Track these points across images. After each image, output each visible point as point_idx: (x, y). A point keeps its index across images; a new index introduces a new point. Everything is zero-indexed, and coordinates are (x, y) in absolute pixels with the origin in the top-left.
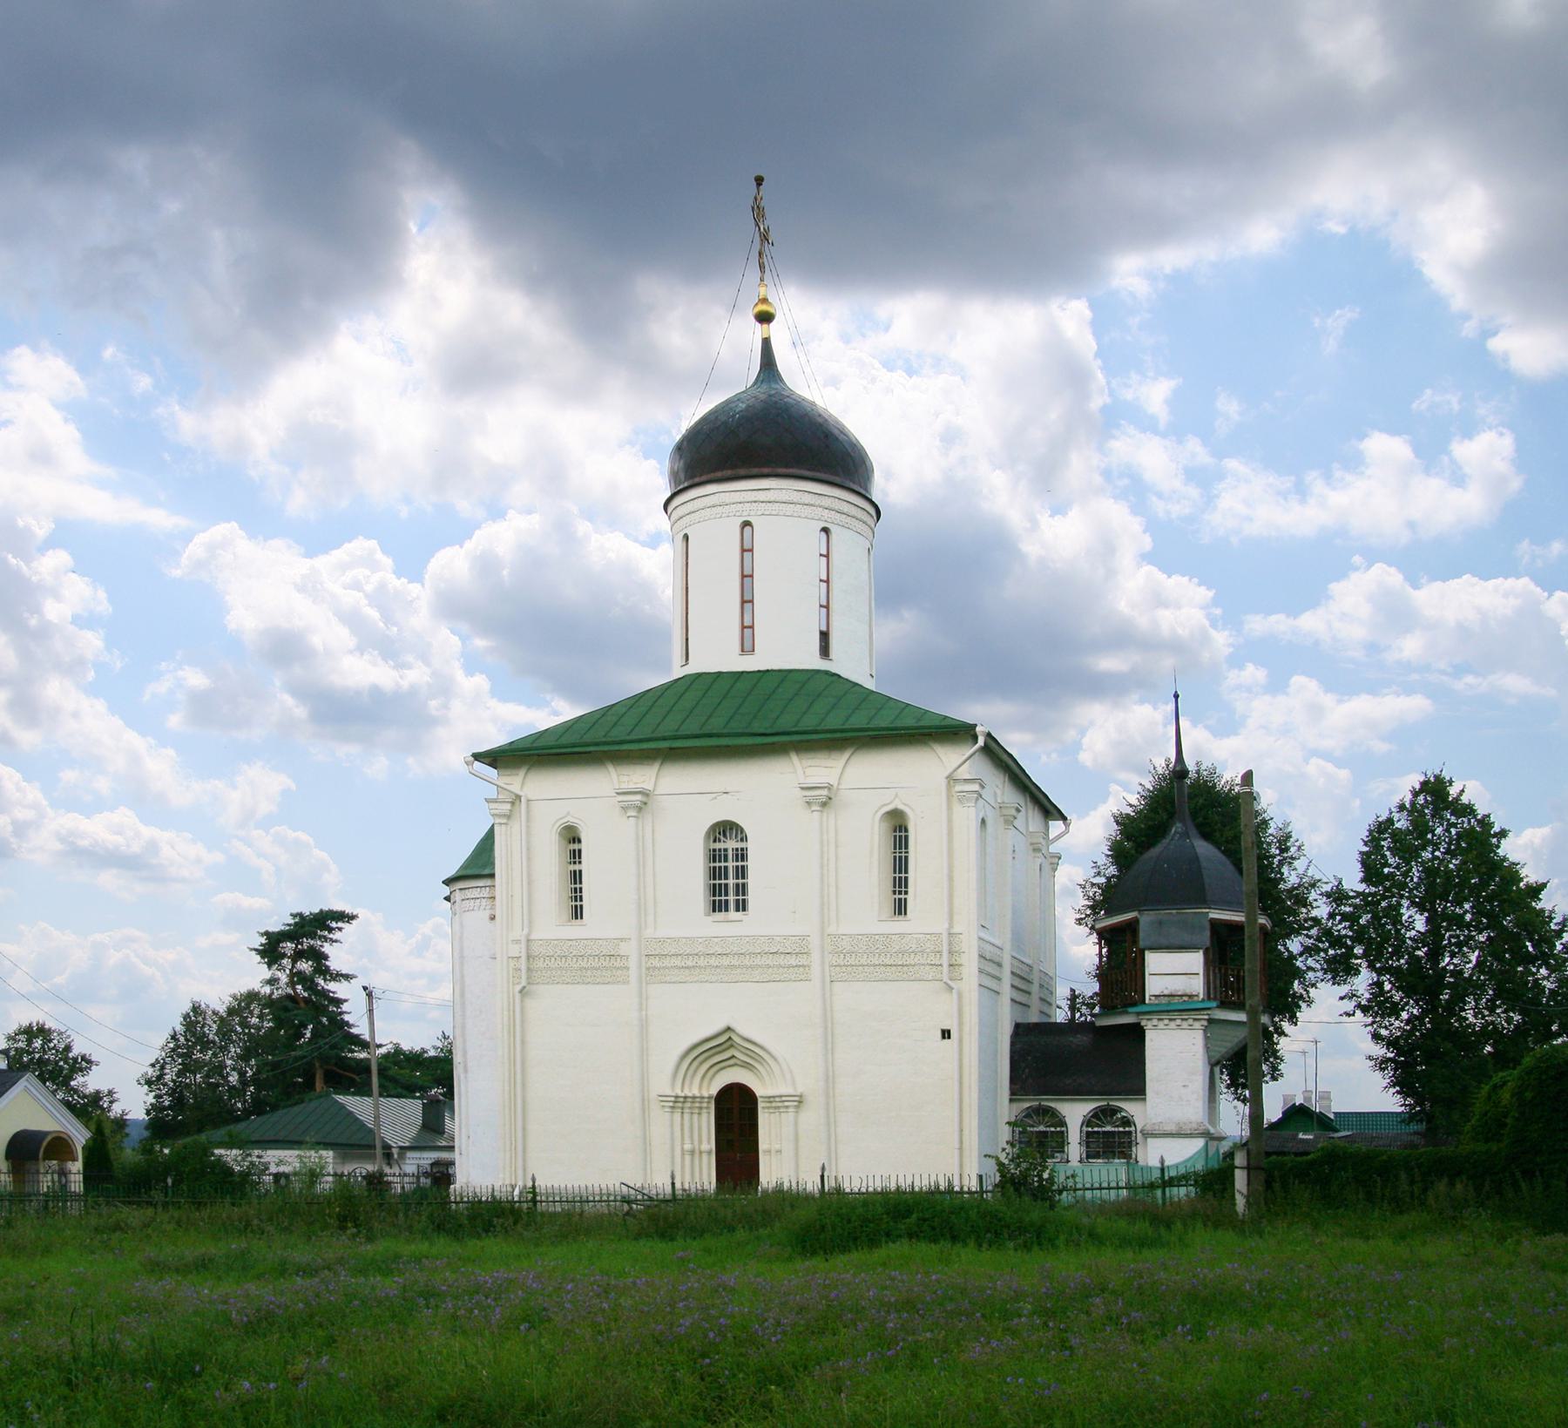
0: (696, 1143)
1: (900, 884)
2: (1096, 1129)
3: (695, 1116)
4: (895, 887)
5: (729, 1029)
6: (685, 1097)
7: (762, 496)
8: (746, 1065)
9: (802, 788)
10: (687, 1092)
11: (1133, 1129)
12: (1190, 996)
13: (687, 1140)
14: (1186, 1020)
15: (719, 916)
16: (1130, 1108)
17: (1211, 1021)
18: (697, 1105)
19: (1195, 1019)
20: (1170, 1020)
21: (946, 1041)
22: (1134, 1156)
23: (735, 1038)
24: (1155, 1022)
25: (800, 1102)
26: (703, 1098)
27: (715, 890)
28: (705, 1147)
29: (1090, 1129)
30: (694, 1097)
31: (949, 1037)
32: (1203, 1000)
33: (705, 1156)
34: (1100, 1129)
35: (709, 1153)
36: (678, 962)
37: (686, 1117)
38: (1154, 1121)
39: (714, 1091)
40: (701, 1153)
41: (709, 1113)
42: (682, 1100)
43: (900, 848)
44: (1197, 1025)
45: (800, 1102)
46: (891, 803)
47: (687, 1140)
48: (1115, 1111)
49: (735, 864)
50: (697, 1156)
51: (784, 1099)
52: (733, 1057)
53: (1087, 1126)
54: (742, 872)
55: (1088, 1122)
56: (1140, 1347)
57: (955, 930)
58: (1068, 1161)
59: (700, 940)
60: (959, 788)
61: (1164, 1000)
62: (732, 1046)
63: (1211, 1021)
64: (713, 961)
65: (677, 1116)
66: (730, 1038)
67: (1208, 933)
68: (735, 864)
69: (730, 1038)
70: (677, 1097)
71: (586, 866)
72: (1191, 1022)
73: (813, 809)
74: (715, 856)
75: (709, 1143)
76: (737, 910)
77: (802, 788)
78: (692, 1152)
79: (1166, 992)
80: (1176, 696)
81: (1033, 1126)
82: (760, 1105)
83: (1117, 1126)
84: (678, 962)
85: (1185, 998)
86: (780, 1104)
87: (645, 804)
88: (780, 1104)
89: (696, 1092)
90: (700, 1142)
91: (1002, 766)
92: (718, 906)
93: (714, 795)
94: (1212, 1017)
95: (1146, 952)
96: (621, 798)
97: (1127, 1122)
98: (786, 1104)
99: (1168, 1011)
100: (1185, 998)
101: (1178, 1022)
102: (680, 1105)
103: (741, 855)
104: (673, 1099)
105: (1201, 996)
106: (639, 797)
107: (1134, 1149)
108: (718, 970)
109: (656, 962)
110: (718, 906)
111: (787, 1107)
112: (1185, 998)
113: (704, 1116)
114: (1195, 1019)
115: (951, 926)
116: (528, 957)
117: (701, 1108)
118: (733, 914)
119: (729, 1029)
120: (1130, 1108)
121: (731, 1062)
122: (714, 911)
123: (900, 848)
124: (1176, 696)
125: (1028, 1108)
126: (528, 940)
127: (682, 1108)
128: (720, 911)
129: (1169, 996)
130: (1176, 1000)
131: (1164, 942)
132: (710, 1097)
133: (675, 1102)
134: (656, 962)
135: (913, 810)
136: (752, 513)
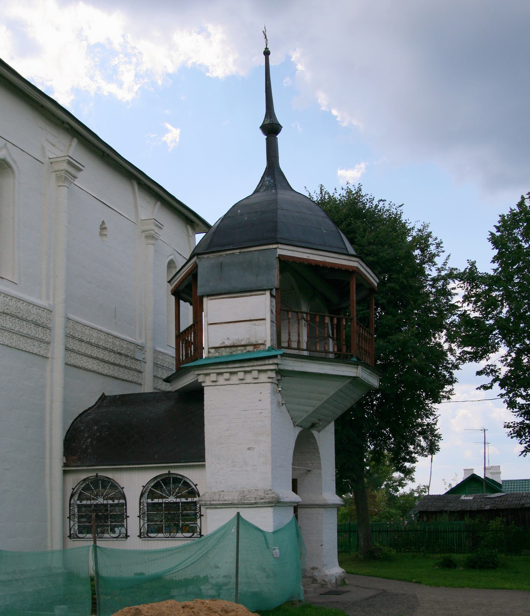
12: (255, 345)
14: (250, 372)
17: (279, 372)
19: (260, 371)
20: (231, 373)
32: (271, 348)
38: (214, 490)
44: (263, 377)
48: (178, 480)
58: (127, 536)
61: (225, 352)
67: (276, 272)
72: (255, 374)
79: (227, 343)
83: (180, 497)
85: (250, 348)
94: (281, 367)
95: (205, 300)
101: (241, 375)
105: (268, 344)
112: (250, 348)
114: (260, 371)
130: (239, 350)
131: (224, 286)
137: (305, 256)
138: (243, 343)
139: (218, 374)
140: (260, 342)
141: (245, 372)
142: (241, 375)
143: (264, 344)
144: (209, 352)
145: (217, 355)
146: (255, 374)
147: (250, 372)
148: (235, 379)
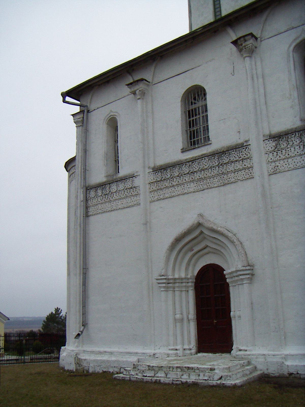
0: (185, 313)
6: (175, 279)
8: (216, 252)
10: (177, 276)
26: (188, 279)
47: (178, 311)
52: (207, 247)
62: (204, 238)
66: (202, 232)
69: (202, 232)
78: (182, 320)
89: (183, 275)
119: (199, 225)
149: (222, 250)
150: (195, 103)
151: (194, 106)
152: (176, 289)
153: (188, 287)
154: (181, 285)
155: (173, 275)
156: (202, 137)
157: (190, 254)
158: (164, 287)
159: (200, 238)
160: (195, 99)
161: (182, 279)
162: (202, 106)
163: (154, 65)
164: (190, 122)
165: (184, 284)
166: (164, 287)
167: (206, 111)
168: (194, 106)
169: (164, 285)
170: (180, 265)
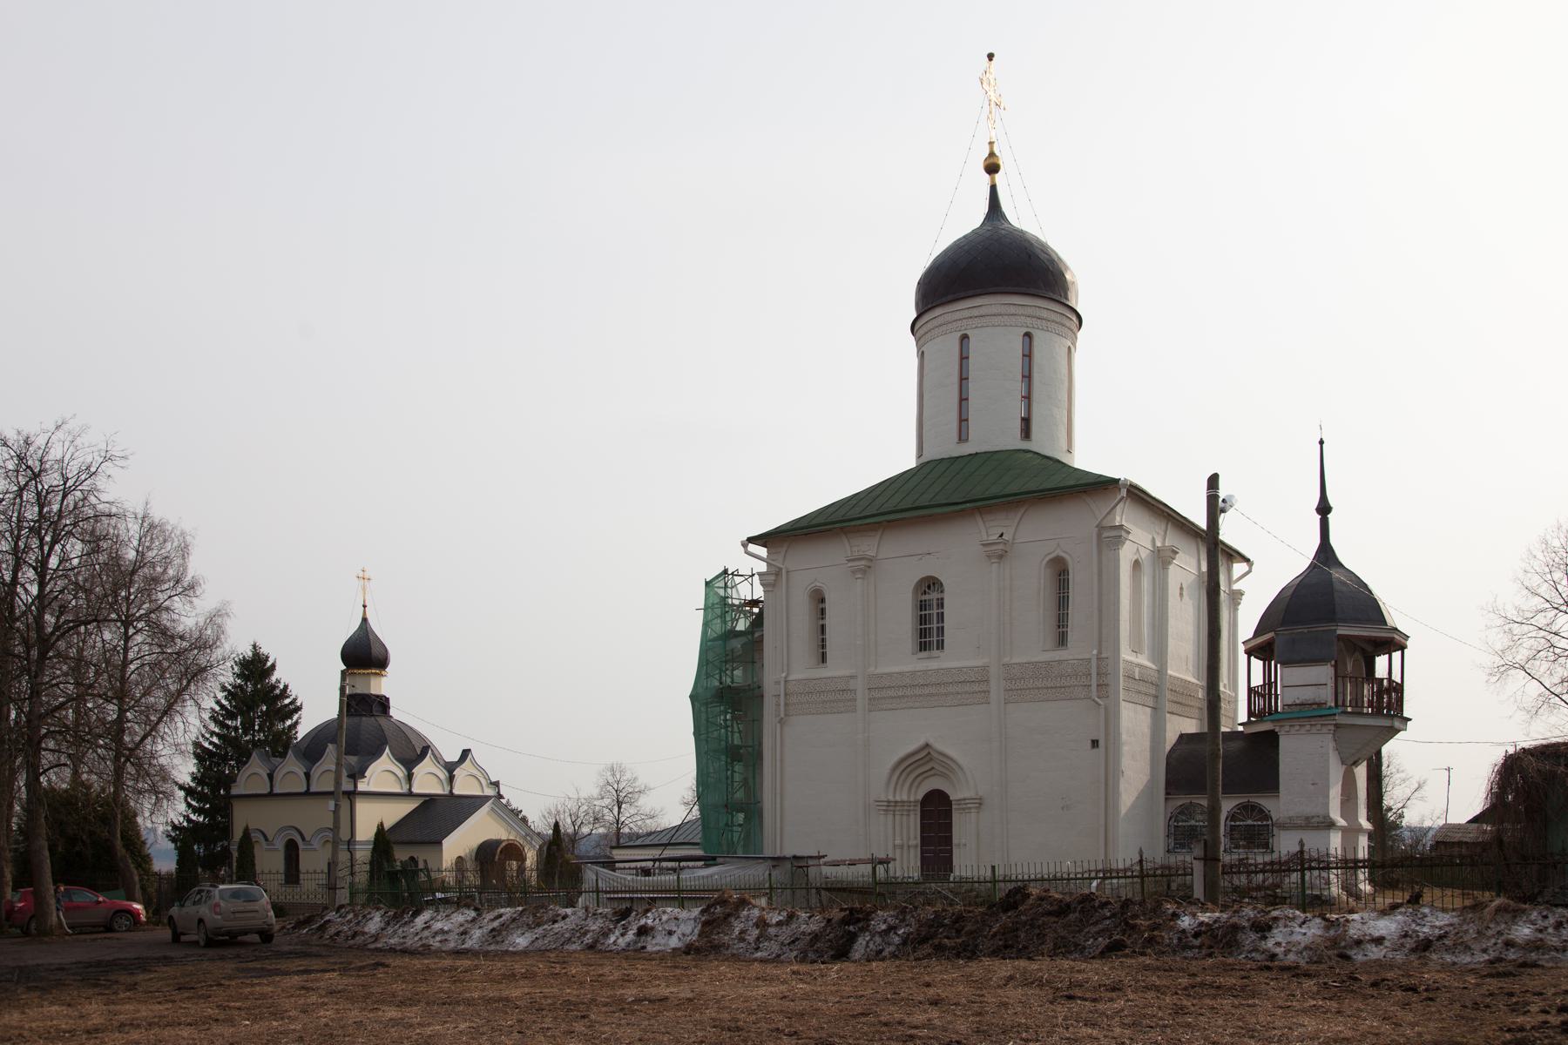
0: (905, 839)
1: (1061, 622)
2: (1238, 823)
3: (905, 818)
4: (1059, 622)
5: (927, 745)
6: (896, 802)
7: (975, 312)
9: (983, 545)
10: (898, 798)
11: (1270, 822)
12: (1319, 704)
13: (898, 838)
14: (1315, 725)
15: (924, 654)
16: (1266, 803)
18: (906, 808)
21: (1095, 750)
22: (1270, 846)
23: (931, 751)
24: (1287, 728)
25: (980, 804)
26: (910, 802)
27: (923, 633)
28: (912, 842)
29: (1233, 823)
30: (903, 802)
31: (1098, 746)
33: (912, 851)
34: (1241, 823)
35: (916, 846)
36: (891, 693)
37: (897, 817)
39: (920, 796)
40: (909, 847)
41: (916, 814)
42: (893, 804)
43: (1064, 589)
44: (1325, 730)
45: (980, 804)
46: (1053, 552)
47: (898, 838)
49: (931, 612)
50: (905, 848)
51: (968, 801)
52: (933, 768)
53: (1231, 821)
54: (941, 617)
55: (1232, 817)
56: (840, 1008)
57: (1103, 656)
59: (908, 674)
60: (1106, 534)
62: (931, 759)
63: (1337, 726)
64: (918, 691)
65: (890, 817)
66: (929, 753)
68: (931, 612)
69: (929, 753)
70: (889, 802)
71: (828, 622)
72: (1319, 727)
73: (993, 561)
74: (923, 606)
75: (915, 839)
76: (938, 649)
77: (983, 545)
78: (902, 847)
79: (1298, 702)
80: (1321, 442)
81: (1186, 821)
82: (954, 807)
84: (891, 693)
86: (964, 806)
87: (869, 567)
88: (964, 806)
89: (905, 798)
90: (909, 839)
91: (1164, 516)
92: (924, 646)
93: (920, 556)
96: (850, 564)
97: (1267, 817)
98: (969, 806)
99: (1299, 718)
100: (1314, 706)
101: (1308, 727)
102: (891, 808)
103: (941, 604)
104: (885, 804)
106: (863, 562)
107: (1271, 840)
108: (921, 698)
109: (876, 694)
110: (924, 646)
111: (970, 808)
113: (912, 816)
115: (1100, 652)
116: (786, 694)
117: (909, 811)
118: (935, 653)
119: (927, 745)
120: (1266, 803)
121: (925, 776)
122: (921, 650)
123: (1064, 589)
124: (1321, 442)
125: (1181, 806)
126: (786, 681)
127: (894, 811)
128: (925, 650)
129: (1299, 705)
132: (915, 802)
133: (888, 806)
134: (876, 694)
135: (1070, 555)
136: (968, 327)
137: (1356, 633)
138: (1310, 702)
139: (1291, 726)
140: (1323, 702)
141: (1311, 725)
142: (1308, 727)
143: (1325, 704)
144: (1283, 709)
145: (1289, 710)
146: (1319, 727)
147: (1315, 725)
148: (1303, 731)
149: (951, 775)
150: (929, 594)
151: (926, 597)
152: (897, 813)
153: (909, 811)
154: (901, 808)
155: (894, 796)
156: (935, 639)
157: (913, 776)
158: (884, 810)
159: (928, 758)
160: (929, 587)
161: (904, 802)
162: (938, 599)
163: (879, 533)
164: (921, 615)
165: (906, 808)
166: (884, 810)
167: (942, 607)
168: (926, 597)
169: (884, 808)
170: (903, 785)
